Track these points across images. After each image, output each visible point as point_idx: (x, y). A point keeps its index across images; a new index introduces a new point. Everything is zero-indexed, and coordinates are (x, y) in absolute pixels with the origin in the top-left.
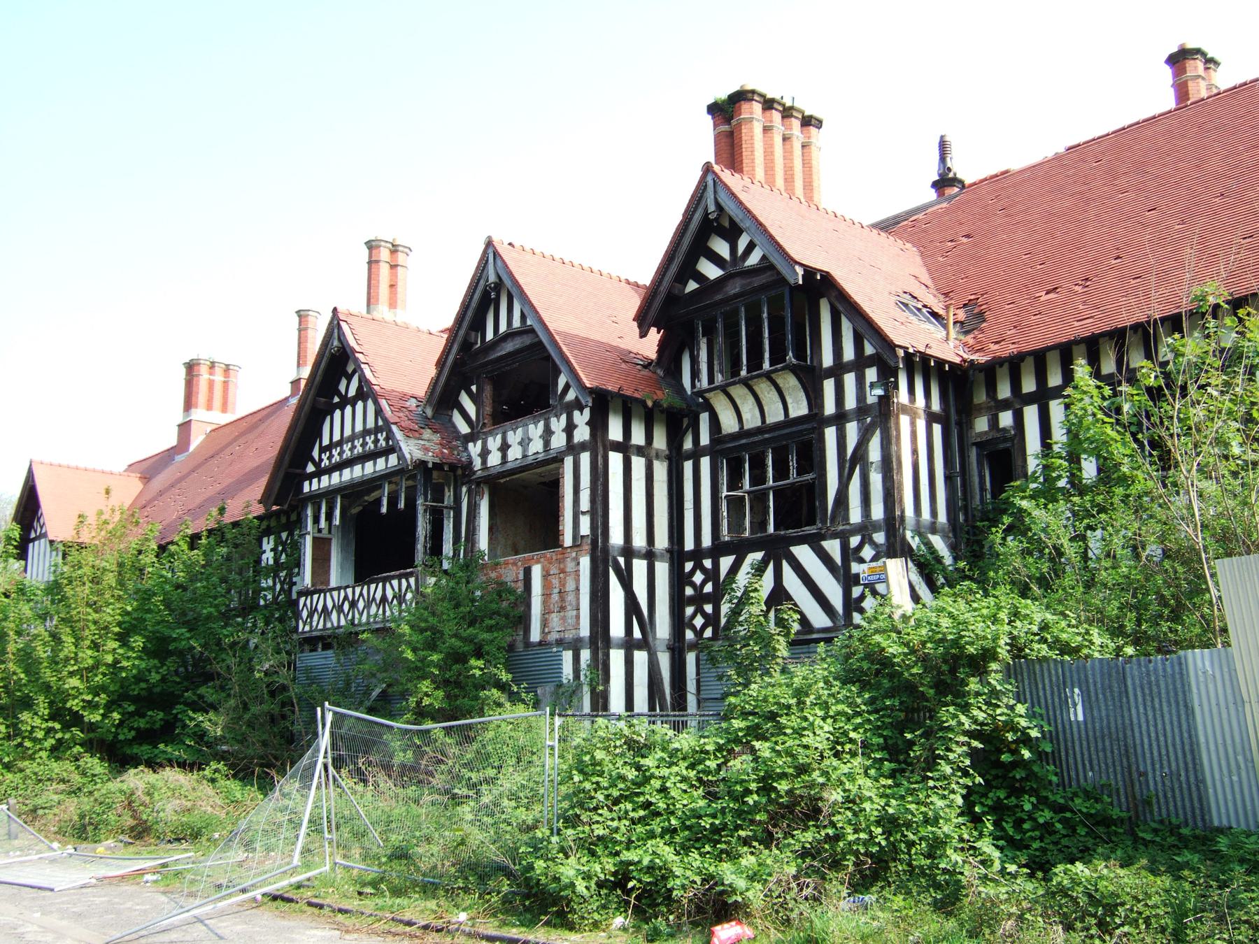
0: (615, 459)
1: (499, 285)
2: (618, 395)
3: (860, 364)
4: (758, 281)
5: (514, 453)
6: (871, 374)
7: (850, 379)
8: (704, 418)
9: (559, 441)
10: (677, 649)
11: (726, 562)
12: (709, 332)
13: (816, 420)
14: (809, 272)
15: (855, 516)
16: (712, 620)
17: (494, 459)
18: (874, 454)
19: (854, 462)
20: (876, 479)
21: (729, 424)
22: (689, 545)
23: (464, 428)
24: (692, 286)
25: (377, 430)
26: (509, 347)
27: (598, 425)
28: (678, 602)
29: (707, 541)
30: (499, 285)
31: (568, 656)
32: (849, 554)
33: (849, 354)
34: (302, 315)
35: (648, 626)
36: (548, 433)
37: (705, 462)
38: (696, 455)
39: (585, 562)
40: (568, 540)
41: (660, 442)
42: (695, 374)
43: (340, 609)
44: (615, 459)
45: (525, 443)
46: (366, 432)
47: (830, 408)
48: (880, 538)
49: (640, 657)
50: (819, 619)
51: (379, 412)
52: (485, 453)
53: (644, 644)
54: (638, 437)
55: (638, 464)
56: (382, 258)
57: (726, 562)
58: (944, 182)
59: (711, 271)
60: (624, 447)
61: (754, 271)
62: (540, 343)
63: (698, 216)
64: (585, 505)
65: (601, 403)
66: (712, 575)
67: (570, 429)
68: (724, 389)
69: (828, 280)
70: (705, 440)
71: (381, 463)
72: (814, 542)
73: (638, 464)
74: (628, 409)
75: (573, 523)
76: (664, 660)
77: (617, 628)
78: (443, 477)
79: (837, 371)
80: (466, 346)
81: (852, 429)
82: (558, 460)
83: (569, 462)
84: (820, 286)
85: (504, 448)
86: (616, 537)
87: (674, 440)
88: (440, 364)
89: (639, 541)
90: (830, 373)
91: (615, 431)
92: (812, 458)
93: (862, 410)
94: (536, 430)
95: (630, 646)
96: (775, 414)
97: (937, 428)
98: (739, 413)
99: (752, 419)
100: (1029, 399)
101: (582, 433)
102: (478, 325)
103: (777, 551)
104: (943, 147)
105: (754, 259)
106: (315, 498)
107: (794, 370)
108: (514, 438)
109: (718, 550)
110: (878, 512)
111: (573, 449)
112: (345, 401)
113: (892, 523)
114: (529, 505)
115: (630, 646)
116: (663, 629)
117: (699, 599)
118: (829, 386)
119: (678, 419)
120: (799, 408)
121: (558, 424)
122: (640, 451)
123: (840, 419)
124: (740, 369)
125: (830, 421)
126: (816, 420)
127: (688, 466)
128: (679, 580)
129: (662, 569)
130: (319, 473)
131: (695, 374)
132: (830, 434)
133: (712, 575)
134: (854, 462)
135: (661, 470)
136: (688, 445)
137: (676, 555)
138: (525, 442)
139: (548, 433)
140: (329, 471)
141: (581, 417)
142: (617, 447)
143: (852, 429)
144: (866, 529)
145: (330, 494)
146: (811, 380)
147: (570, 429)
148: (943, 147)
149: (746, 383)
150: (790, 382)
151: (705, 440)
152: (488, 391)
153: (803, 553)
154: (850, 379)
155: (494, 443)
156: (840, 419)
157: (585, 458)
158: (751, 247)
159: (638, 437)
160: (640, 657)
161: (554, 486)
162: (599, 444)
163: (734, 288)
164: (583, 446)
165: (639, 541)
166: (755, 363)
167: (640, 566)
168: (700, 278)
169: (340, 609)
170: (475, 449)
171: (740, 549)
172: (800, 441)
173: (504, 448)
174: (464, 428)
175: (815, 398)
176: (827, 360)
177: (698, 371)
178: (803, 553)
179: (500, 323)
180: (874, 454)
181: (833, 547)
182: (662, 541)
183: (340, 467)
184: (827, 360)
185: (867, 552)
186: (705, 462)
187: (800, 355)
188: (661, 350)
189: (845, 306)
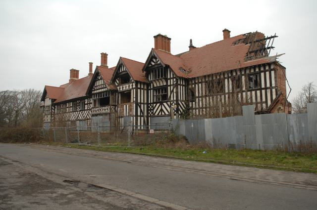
0: (139, 90)
1: (122, 64)
2: (140, 81)
3: (173, 78)
4: (159, 66)
5: (124, 89)
6: (175, 80)
7: (172, 80)
8: (152, 84)
9: (131, 87)
10: (148, 117)
11: (154, 105)
12: (153, 72)
13: (167, 85)
14: (166, 65)
15: (172, 99)
16: (152, 113)
17: (121, 89)
18: (175, 91)
19: (172, 92)
20: (175, 94)
21: (155, 85)
22: (149, 102)
23: (117, 85)
24: (150, 65)
25: (104, 84)
26: (123, 73)
27: (136, 85)
28: (148, 110)
29: (152, 102)
30: (122, 64)
31: (132, 118)
32: (171, 104)
33: (172, 77)
34: (91, 64)
35: (143, 113)
36: (129, 86)
37: (152, 91)
38: (150, 90)
39: (134, 105)
40: (132, 101)
41: (145, 88)
42: (151, 78)
43: (98, 110)
44: (139, 90)
45: (126, 87)
46: (102, 85)
47: (169, 84)
48: (175, 102)
49: (142, 118)
50: (167, 113)
51: (104, 82)
52: (120, 88)
53: (143, 116)
54: (142, 87)
55: (142, 91)
56: (104, 57)
57: (154, 105)
58: (191, 47)
59: (153, 64)
60: (140, 88)
61: (159, 64)
62: (128, 73)
63: (151, 56)
64: (134, 96)
65: (137, 82)
66: (152, 107)
67: (132, 86)
68: (154, 81)
69: (169, 66)
70: (152, 87)
71: (104, 89)
72: (166, 102)
73: (142, 91)
74: (141, 83)
75: (133, 99)
76: (146, 118)
77: (139, 114)
78: (114, 92)
79: (170, 79)
80: (117, 72)
81: (172, 87)
82: (131, 90)
83: (132, 90)
84: (167, 67)
85: (123, 88)
86: (139, 101)
87: (148, 87)
88: (113, 75)
89: (142, 102)
90: (169, 79)
91: (139, 86)
92: (166, 90)
93: (173, 85)
94: (127, 86)
95: (141, 116)
96: (162, 85)
97: (184, 87)
98: (157, 84)
99: (158, 85)
100: (200, 83)
101: (134, 86)
102: (119, 70)
103: (161, 104)
104: (191, 41)
105: (159, 62)
106: (94, 94)
107: (164, 78)
108: (124, 86)
109: (154, 103)
110: (175, 99)
111: (133, 89)
112: (98, 80)
113: (177, 100)
114: (126, 96)
115: (141, 116)
116: (145, 114)
117: (151, 110)
118: (169, 81)
119: (148, 85)
120: (165, 84)
121: (131, 85)
122: (142, 89)
123: (170, 86)
124: (157, 78)
125: (169, 86)
126: (167, 85)
127: (149, 91)
128: (148, 107)
129: (145, 106)
130: (95, 90)
131: (151, 78)
132: (169, 87)
133: (152, 107)
134: (172, 92)
135: (145, 92)
136: (149, 88)
137: (148, 104)
138: (125, 87)
139: (129, 86)
140: (96, 90)
141: (134, 84)
142: (139, 88)
143: (172, 87)
144: (173, 101)
145: (96, 94)
146: (167, 80)
147: (132, 86)
148: (191, 41)
149: (158, 80)
150: (164, 80)
151: (152, 87)
152: (120, 79)
153: (165, 104)
154: (172, 80)
155: (121, 87)
156: (170, 86)
157: (135, 90)
158: (158, 61)
159: (142, 87)
160: (142, 118)
161: (130, 93)
162: (137, 88)
163: (156, 66)
164: (134, 88)
165: (142, 102)
166: (159, 77)
167: (142, 105)
168: (151, 64)
169: (98, 110)
170: (118, 88)
171: (156, 103)
172: (165, 88)
173: (123, 88)
174: (117, 85)
175: (167, 82)
176: (169, 77)
177: (151, 78)
178: (165, 104)
179: (123, 69)
180: (175, 91)
181: (169, 103)
182: (145, 102)
183: (98, 89)
184: (169, 77)
185: (173, 104)
186: (152, 91)
187: (165, 76)
188: (146, 74)
189: (171, 70)
